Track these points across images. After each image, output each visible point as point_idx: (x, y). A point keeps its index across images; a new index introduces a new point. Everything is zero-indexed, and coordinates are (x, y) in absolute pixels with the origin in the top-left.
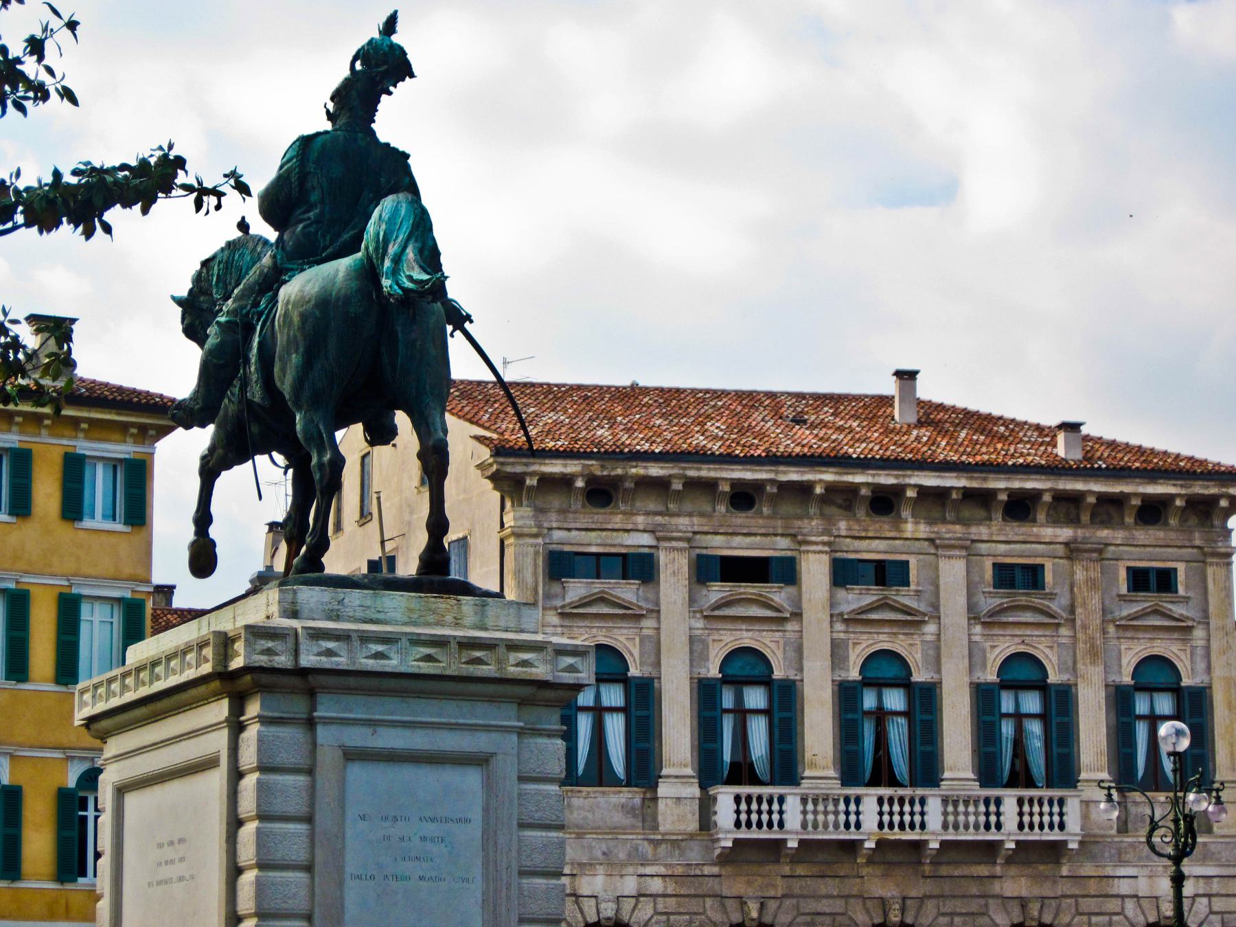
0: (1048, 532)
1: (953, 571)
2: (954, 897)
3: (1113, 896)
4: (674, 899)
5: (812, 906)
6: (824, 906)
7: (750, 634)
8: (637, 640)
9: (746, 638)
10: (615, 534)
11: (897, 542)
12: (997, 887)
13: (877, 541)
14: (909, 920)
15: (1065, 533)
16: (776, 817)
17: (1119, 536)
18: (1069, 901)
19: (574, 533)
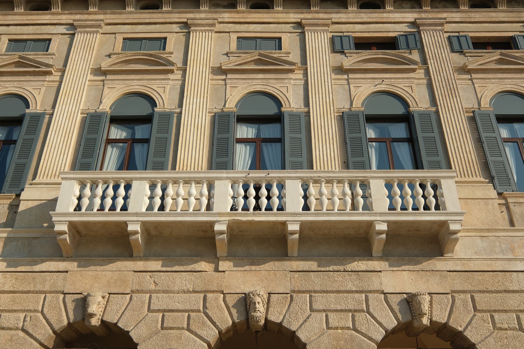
0: (398, 16)
1: (318, 42)
2: (327, 292)
3: (513, 292)
4: (10, 295)
5: (161, 301)
6: (177, 302)
7: (140, 83)
8: (43, 89)
9: (136, 84)
10: (44, 27)
11: (272, 25)
12: (375, 282)
13: (255, 25)
14: (275, 317)
15: (410, 16)
16: (120, 202)
17: (456, 16)
18: (462, 296)
19: (11, 27)
